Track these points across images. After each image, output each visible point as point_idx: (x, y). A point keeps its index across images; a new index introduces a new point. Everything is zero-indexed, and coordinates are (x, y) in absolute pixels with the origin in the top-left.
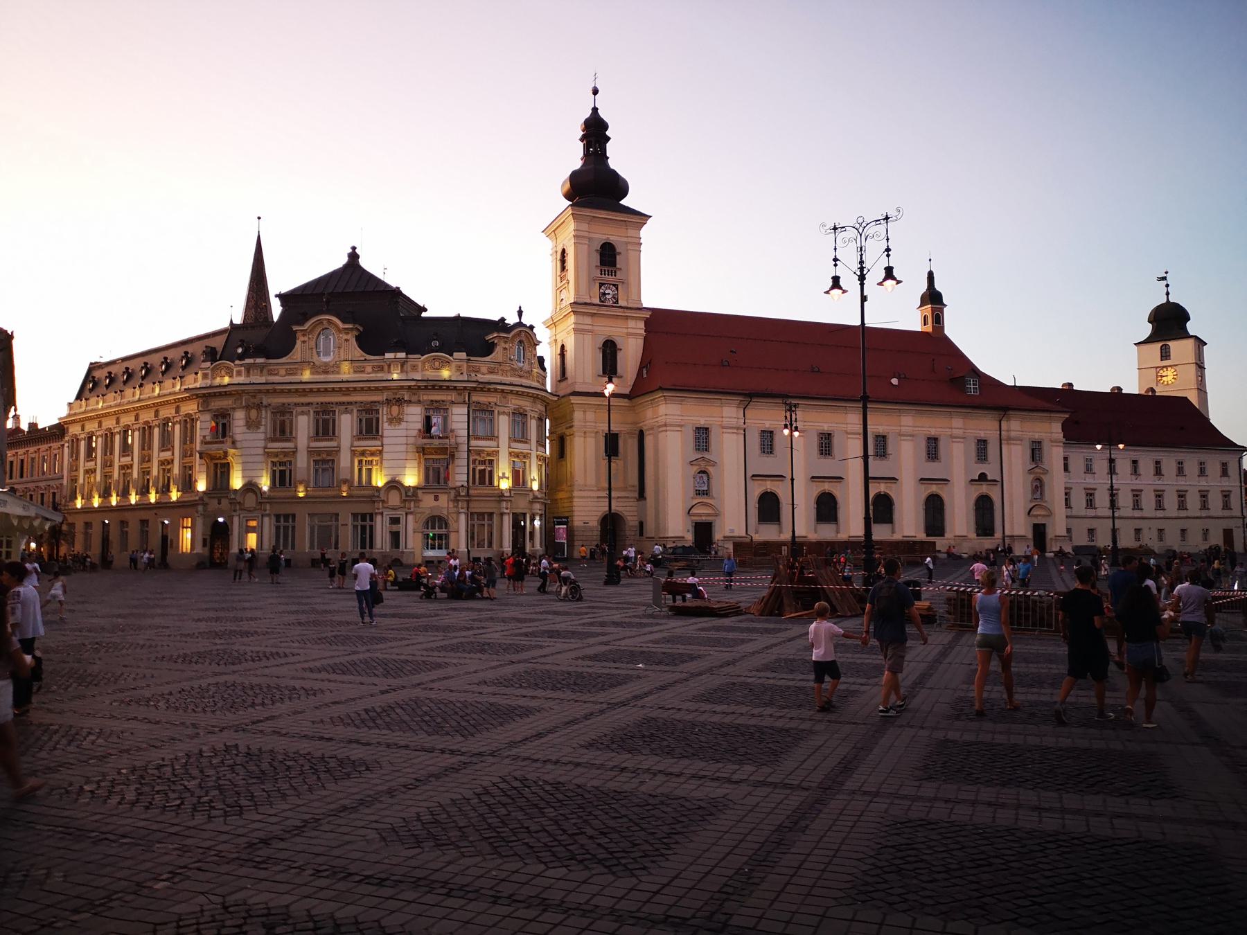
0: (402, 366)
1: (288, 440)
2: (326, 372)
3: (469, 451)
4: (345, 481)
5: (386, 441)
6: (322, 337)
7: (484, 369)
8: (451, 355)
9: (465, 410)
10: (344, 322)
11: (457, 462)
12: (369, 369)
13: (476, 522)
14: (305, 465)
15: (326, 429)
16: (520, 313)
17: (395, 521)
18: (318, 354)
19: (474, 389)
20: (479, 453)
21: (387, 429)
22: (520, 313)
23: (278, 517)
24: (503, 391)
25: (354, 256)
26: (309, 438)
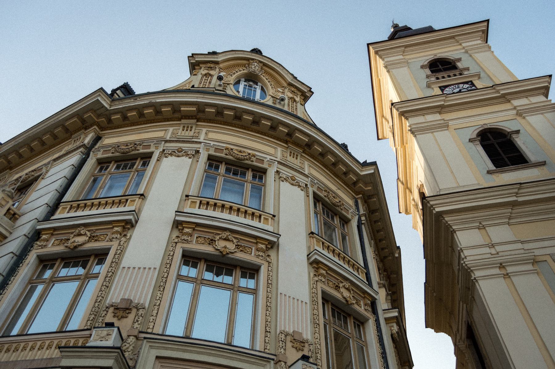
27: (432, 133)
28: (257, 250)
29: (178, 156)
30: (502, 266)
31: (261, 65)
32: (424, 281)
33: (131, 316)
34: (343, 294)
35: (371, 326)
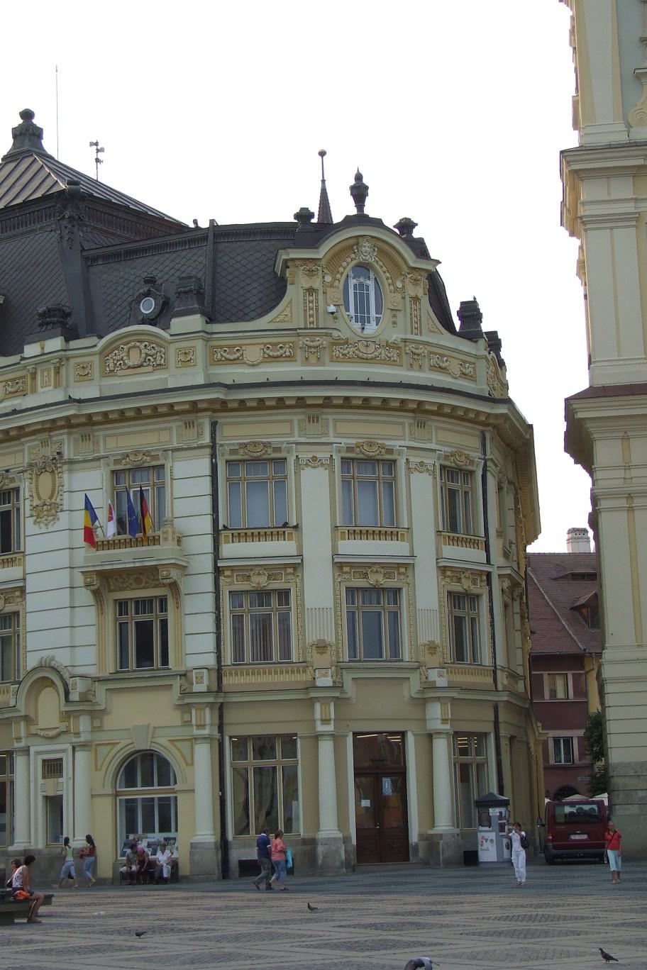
0: (57, 372)
3: (218, 571)
5: (32, 563)
7: (253, 353)
8: (166, 327)
9: (204, 465)
11: (189, 604)
13: (251, 762)
16: (359, 192)
17: (53, 768)
19: (223, 406)
20: (244, 571)
22: (359, 192)
24: (301, 403)
25: (28, 133)
27: (611, 229)
28: (399, 574)
29: (314, 467)
30: (630, 497)
31: (374, 241)
32: (565, 430)
33: (329, 652)
34: (466, 584)
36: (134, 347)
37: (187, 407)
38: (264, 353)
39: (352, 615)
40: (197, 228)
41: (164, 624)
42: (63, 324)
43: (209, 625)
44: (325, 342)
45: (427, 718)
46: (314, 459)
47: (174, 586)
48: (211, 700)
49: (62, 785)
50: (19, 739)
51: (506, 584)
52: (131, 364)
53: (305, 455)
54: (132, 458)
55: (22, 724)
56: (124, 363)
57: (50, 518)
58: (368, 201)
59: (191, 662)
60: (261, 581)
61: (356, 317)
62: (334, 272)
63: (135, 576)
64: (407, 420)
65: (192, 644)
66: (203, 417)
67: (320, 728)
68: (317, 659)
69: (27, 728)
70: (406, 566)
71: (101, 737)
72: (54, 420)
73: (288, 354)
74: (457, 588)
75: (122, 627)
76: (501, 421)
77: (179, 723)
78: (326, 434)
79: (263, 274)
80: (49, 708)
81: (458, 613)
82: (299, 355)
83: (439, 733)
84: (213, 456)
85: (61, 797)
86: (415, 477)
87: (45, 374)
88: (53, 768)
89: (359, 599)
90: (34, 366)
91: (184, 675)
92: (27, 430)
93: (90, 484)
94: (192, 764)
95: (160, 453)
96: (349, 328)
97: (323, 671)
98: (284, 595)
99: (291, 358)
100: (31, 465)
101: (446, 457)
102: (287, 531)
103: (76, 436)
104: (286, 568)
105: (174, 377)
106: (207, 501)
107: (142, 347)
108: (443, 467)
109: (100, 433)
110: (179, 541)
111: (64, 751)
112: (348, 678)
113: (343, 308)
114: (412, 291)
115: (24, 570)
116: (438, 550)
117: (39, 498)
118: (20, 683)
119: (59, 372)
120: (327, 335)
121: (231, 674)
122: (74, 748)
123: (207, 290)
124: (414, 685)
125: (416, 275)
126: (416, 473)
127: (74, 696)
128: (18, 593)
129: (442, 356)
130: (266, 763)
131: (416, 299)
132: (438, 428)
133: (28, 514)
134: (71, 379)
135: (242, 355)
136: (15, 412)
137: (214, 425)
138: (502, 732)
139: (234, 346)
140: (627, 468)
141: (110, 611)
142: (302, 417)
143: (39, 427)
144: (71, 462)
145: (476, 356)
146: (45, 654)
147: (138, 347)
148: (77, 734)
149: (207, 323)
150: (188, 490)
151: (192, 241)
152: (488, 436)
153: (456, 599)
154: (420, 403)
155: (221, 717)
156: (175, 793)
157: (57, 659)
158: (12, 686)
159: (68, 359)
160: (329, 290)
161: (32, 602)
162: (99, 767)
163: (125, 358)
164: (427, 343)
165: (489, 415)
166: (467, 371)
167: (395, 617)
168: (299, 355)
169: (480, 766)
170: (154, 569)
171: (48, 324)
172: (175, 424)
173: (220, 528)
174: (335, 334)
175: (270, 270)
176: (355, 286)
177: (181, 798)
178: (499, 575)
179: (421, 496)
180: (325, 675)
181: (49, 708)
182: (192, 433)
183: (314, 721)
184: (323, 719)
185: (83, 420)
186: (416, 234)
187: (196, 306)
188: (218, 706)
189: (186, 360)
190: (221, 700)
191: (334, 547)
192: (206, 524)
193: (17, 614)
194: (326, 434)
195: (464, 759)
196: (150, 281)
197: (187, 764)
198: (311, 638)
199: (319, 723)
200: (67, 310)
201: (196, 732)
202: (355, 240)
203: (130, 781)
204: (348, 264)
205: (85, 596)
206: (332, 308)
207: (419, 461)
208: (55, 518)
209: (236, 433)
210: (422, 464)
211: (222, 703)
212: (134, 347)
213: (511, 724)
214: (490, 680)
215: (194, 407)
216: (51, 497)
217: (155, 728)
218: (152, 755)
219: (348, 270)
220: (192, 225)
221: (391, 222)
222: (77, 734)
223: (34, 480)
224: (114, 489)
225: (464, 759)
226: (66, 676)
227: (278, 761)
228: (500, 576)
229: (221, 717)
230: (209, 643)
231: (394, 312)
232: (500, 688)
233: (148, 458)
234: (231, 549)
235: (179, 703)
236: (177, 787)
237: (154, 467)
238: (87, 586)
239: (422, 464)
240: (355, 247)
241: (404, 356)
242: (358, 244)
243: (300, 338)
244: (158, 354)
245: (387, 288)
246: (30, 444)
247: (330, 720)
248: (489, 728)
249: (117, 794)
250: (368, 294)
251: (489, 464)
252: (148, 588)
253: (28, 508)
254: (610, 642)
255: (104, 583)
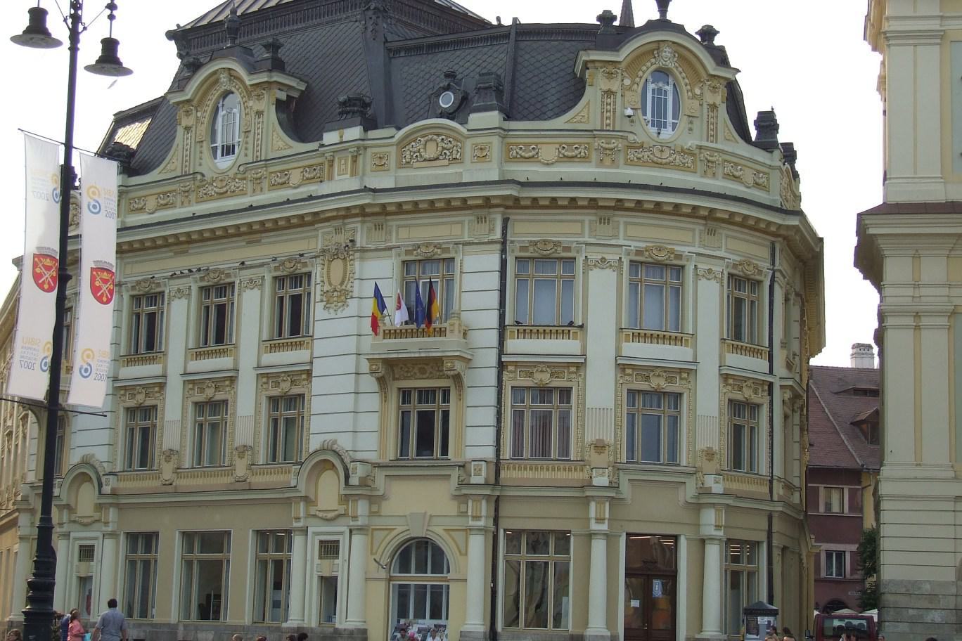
0: (355, 160)
1: (152, 360)
2: (222, 195)
3: (501, 366)
4: (243, 450)
5: (319, 348)
6: (221, 113)
7: (548, 152)
9: (492, 260)
10: (253, 69)
11: (472, 397)
12: (295, 177)
13: (524, 556)
14: (178, 416)
15: (217, 328)
17: (329, 549)
18: (215, 158)
19: (516, 203)
20: (528, 367)
21: (322, 321)
23: (133, 538)
24: (593, 204)
26: (187, 349)
27: (915, 45)
28: (681, 379)
30: (917, 315)
31: (675, 48)
33: (607, 452)
34: (747, 394)
35: (765, 411)
36: (431, 140)
37: (480, 202)
38: (560, 152)
39: (631, 417)
40: (500, 25)
41: (446, 414)
42: (363, 114)
43: (489, 416)
44: (620, 145)
45: (701, 523)
46: (603, 260)
47: (458, 378)
48: (488, 492)
49: (337, 567)
50: (298, 519)
51: (788, 395)
52: (427, 156)
53: (595, 255)
54: (424, 249)
55: (302, 505)
56: (421, 155)
57: (340, 304)
58: (671, 7)
59: (470, 454)
60: (543, 378)
61: (653, 121)
62: (633, 76)
63: (420, 366)
64: (698, 227)
65: (472, 436)
66: (496, 213)
67: (594, 526)
68: (595, 458)
69: (307, 510)
70: (688, 371)
71: (378, 522)
72: (348, 208)
73: (583, 154)
74: (738, 396)
75: (405, 416)
76: (791, 233)
77: (455, 513)
78: (616, 237)
79: (562, 74)
80: (329, 490)
81: (737, 421)
82: (594, 156)
83: (712, 539)
84: (503, 251)
85: (336, 578)
86: (703, 283)
87: (343, 162)
88: (329, 549)
89: (640, 401)
90: (332, 154)
91: (462, 466)
92: (322, 216)
93: (381, 272)
94: (466, 554)
95: (451, 246)
96: (645, 132)
97: (601, 471)
98: (566, 393)
99: (585, 159)
100: (323, 251)
101: (735, 266)
102: (573, 330)
103: (369, 225)
104: (569, 367)
105: (470, 172)
106: (495, 296)
107: (439, 140)
108: (731, 275)
109: (393, 222)
110: (465, 334)
111: (341, 533)
112: (624, 479)
113: (640, 112)
114: (710, 98)
115: (312, 353)
116: (721, 357)
117: (330, 284)
118: (301, 464)
119: (355, 161)
120: (622, 137)
121: (508, 468)
122: (351, 531)
123: (507, 87)
124: (690, 490)
125: (715, 83)
126: (704, 280)
127: (354, 481)
128: (304, 376)
129: (736, 164)
130: (539, 557)
131: (713, 107)
132: (727, 236)
133: (318, 298)
134: (368, 168)
135: (537, 153)
136: (311, 198)
137: (506, 221)
138: (775, 542)
139: (530, 144)
140: (916, 286)
141: (394, 399)
142: (594, 218)
143: (335, 214)
144: (363, 250)
145: (770, 167)
146: (328, 437)
147: (435, 140)
148: (355, 518)
149: (504, 119)
150: (476, 283)
151: (494, 38)
152: (778, 247)
153: (737, 407)
154: (712, 210)
155: (497, 510)
156: (448, 581)
157: (339, 442)
158: (293, 467)
159: (365, 148)
160: (628, 94)
161: (317, 385)
162: (374, 551)
163: (422, 150)
164: (722, 151)
165: (780, 226)
166: (760, 181)
167: (675, 422)
168: (594, 156)
169: (751, 575)
170: (438, 361)
171: (348, 113)
172: (467, 218)
173: (506, 324)
174: (631, 137)
175: (570, 70)
176: (653, 90)
177: (452, 586)
178: (780, 386)
179: (707, 303)
180: (602, 475)
181: (329, 490)
182: (484, 227)
183: (588, 519)
184: (597, 518)
185: (377, 209)
186: (718, 41)
187: (495, 102)
188: (495, 498)
189: (482, 155)
190: (498, 493)
191: (618, 349)
192: (492, 319)
193: (302, 396)
194: (616, 237)
195: (736, 566)
196: (451, 75)
197: (461, 554)
198: (590, 437)
199: (593, 521)
200: (367, 100)
201: (471, 523)
202: (654, 46)
203: (404, 568)
204: (648, 68)
205: (370, 383)
206: (629, 112)
207: (707, 268)
208: (345, 304)
209: (528, 230)
210: (710, 271)
211: (499, 496)
212: (431, 140)
213: (787, 536)
214: (766, 489)
215: (487, 203)
216: (342, 284)
217: (431, 516)
218: (427, 543)
219: (647, 75)
220: (495, 22)
221: (692, 28)
222: (355, 518)
223: (326, 267)
224: (403, 279)
225: (736, 566)
226: (347, 460)
227: (551, 556)
228: (782, 387)
229: (497, 510)
230: (489, 436)
231: (690, 119)
232: (775, 498)
233: (439, 250)
234: (517, 345)
235: (457, 493)
236: (449, 576)
237: (444, 259)
238: (372, 373)
239: (710, 271)
240: (655, 52)
241: (699, 163)
242: (658, 49)
243: (596, 139)
244: (455, 148)
245: (685, 94)
246: (323, 230)
247: (604, 519)
248: (762, 537)
249: (390, 579)
250: (666, 100)
251: (777, 274)
252: (431, 378)
253: (318, 293)
254: (888, 459)
255: (389, 371)
